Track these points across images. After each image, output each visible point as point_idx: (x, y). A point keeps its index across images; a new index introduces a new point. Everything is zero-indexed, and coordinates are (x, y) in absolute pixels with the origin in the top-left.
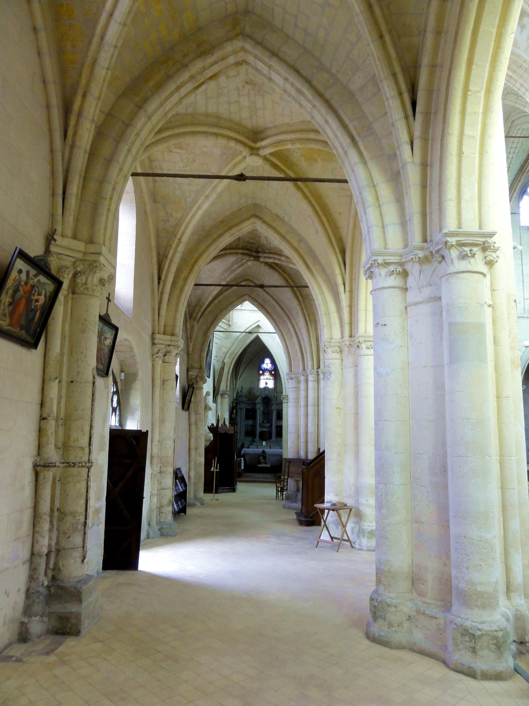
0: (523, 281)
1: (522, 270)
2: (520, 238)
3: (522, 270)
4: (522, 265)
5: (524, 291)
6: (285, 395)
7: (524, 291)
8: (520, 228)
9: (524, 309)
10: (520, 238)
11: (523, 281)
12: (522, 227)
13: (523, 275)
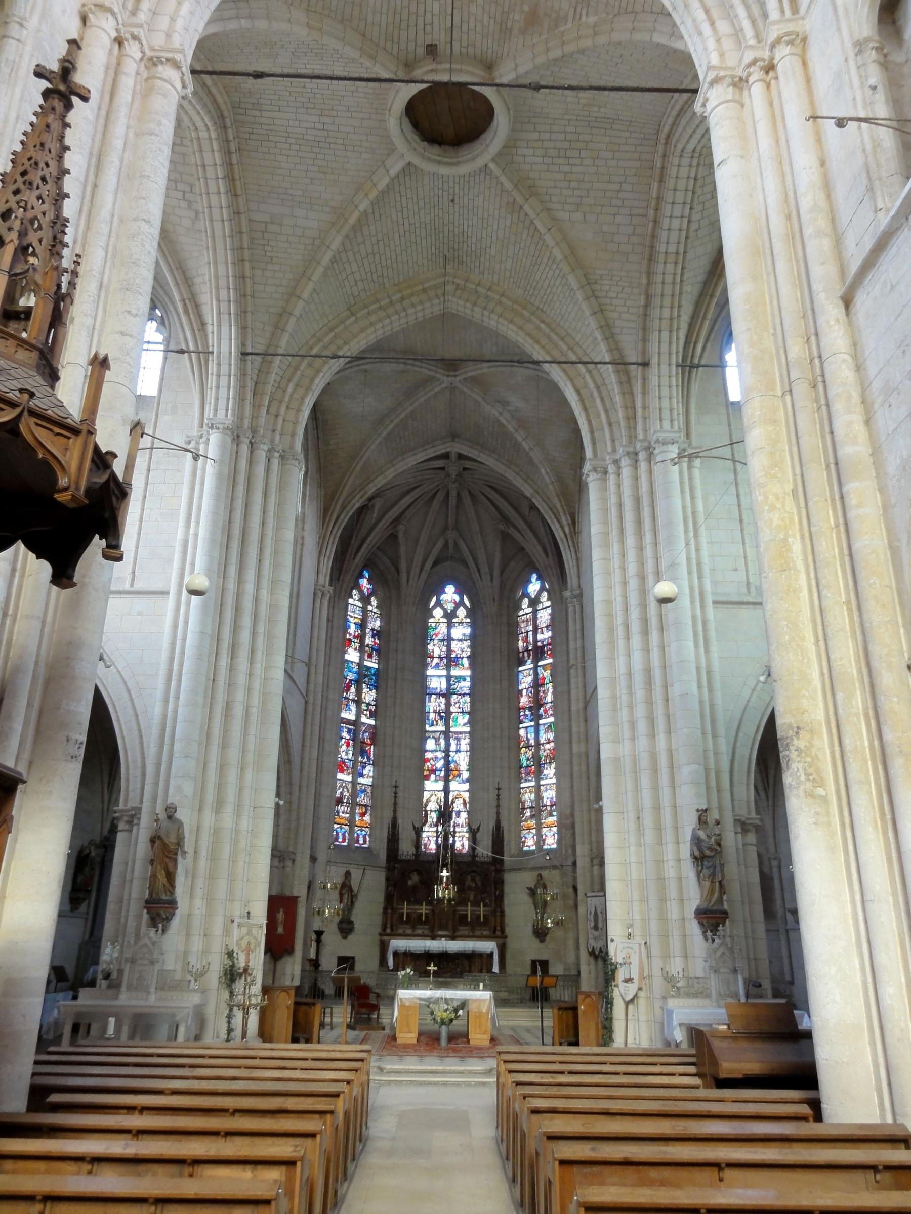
0: (741, 521)
1: (738, 496)
2: (729, 425)
3: (738, 496)
4: (737, 485)
5: (744, 544)
6: (121, 811)
7: (744, 544)
8: (727, 406)
9: (748, 584)
10: (729, 425)
11: (741, 521)
12: (733, 403)
13: (739, 506)
